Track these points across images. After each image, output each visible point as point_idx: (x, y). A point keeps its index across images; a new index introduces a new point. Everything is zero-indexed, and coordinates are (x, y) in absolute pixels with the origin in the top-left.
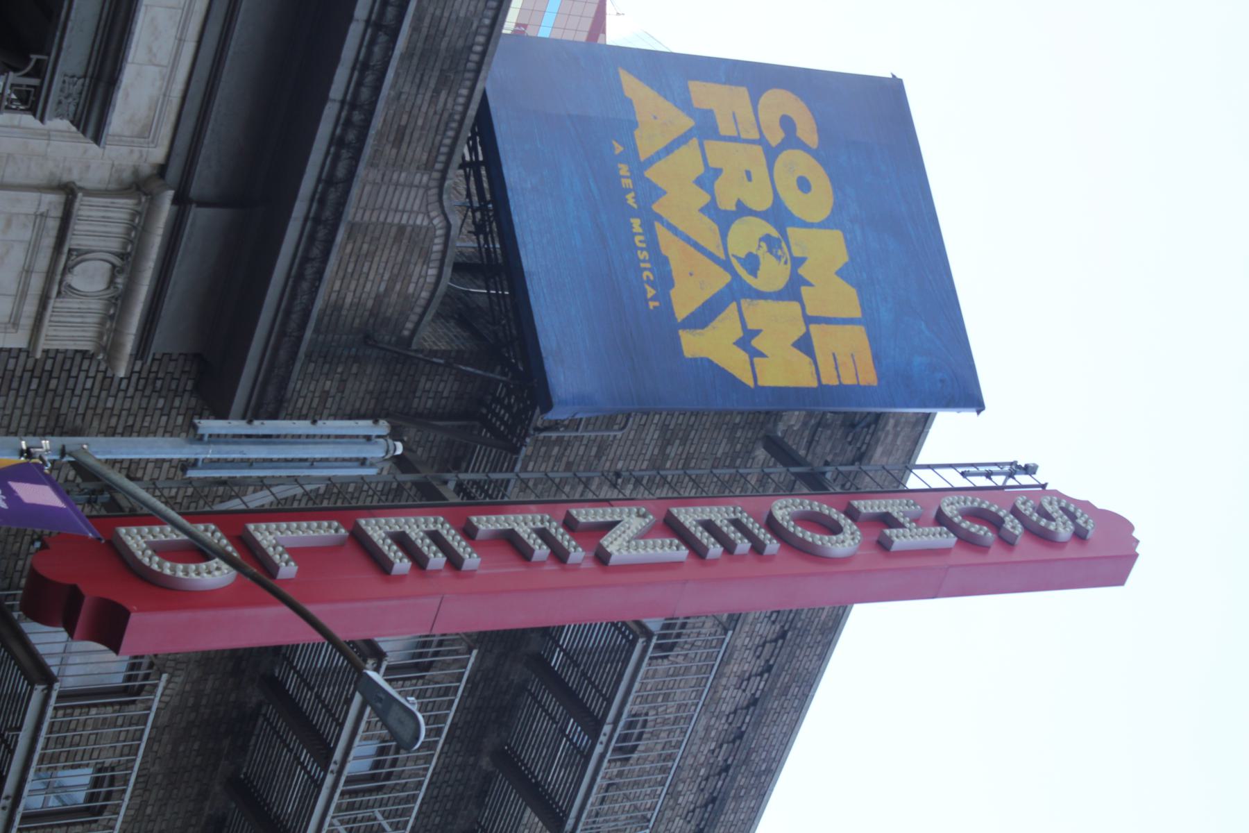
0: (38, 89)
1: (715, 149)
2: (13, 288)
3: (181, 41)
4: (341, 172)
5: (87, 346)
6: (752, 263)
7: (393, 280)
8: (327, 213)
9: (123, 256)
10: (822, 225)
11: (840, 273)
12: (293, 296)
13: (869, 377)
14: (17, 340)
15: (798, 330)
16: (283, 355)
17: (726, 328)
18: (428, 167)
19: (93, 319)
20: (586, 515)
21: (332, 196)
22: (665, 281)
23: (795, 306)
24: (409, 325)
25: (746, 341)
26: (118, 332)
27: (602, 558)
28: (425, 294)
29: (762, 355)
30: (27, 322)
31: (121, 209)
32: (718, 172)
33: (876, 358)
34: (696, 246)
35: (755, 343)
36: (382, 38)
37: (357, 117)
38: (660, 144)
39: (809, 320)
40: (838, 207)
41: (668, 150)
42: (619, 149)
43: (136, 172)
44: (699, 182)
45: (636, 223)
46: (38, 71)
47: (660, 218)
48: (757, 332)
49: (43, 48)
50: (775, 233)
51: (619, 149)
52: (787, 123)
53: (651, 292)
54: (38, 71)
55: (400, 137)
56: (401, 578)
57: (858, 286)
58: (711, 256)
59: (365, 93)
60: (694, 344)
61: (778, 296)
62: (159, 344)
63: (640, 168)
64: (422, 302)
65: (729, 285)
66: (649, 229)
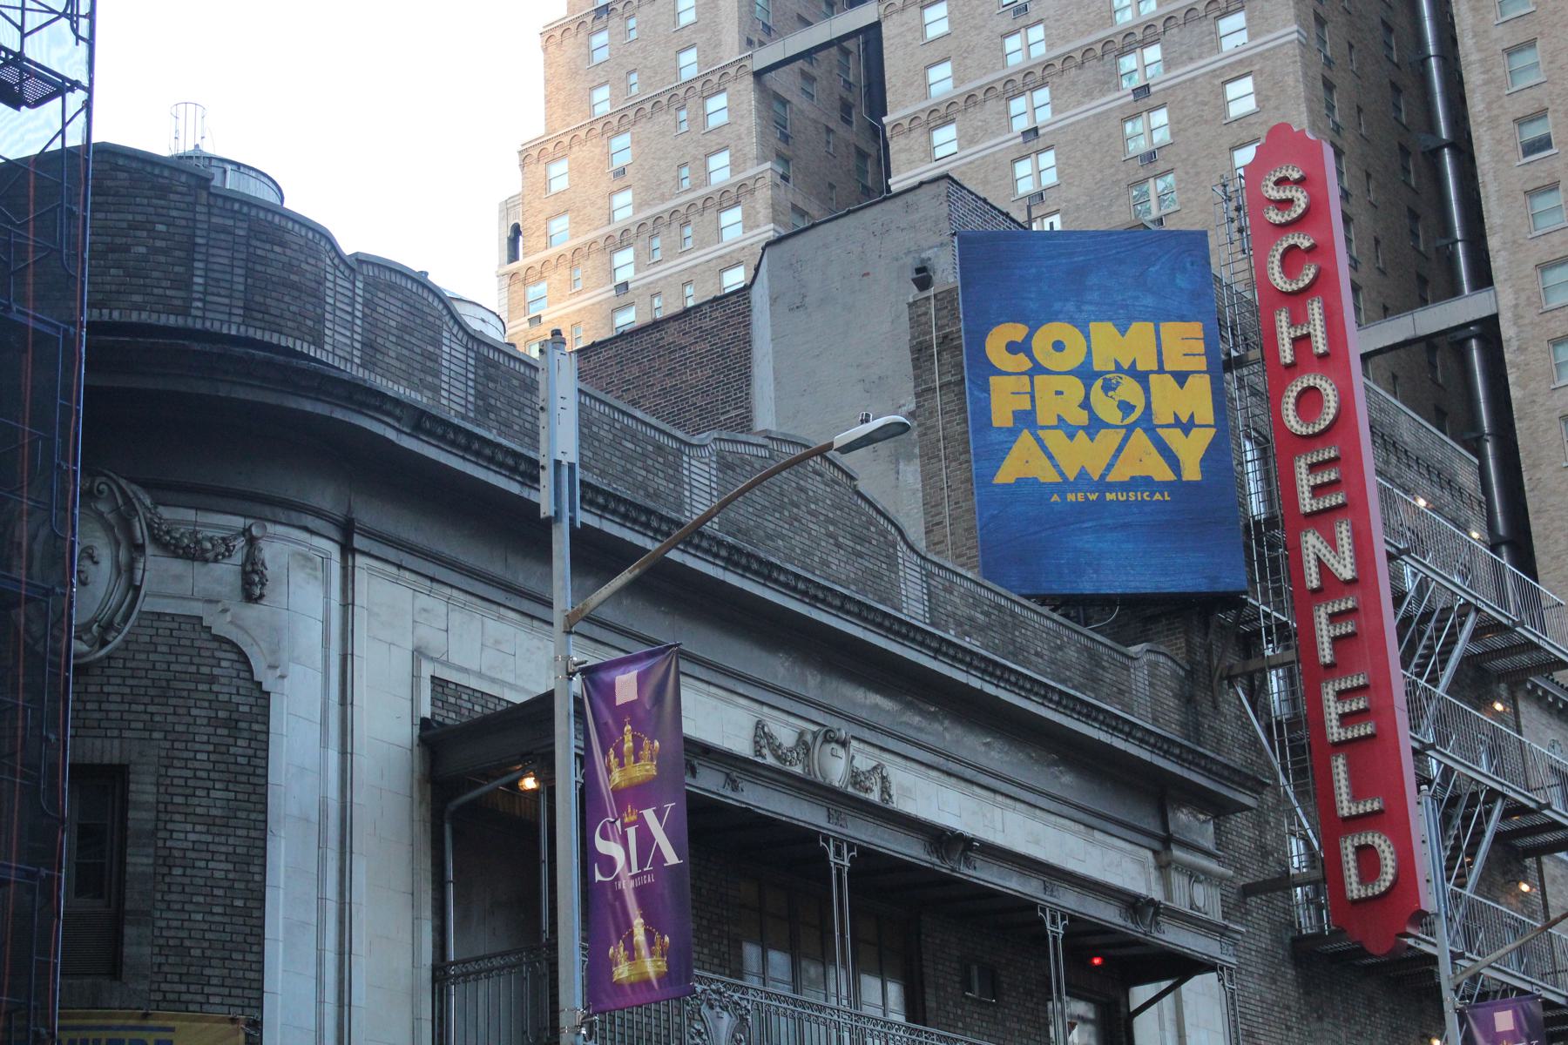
1: (1045, 416)
3: (1114, 847)
4: (1177, 751)
6: (1126, 407)
7: (1168, 687)
9: (1191, 877)
10: (1087, 337)
11: (1123, 332)
12: (1216, 774)
13: (1196, 329)
15: (1171, 382)
17: (1173, 437)
18: (1127, 668)
20: (1313, 581)
22: (1146, 482)
23: (1152, 377)
25: (1187, 427)
27: (1353, 582)
29: (1192, 416)
31: (1178, 880)
32: (1060, 418)
33: (1182, 318)
34: (1120, 450)
35: (1184, 420)
38: (1047, 463)
39: (1161, 370)
40: (1072, 321)
41: (1050, 457)
42: (1055, 498)
44: (1071, 436)
45: (1110, 496)
47: (1103, 476)
48: (1176, 417)
50: (1099, 382)
51: (1055, 498)
52: (1013, 348)
53: (1158, 496)
55: (1121, 692)
56: (1378, 727)
57: (1132, 319)
58: (1125, 439)
59: (1152, 740)
60: (1192, 472)
61: (1147, 390)
62: (1208, 842)
63: (1064, 485)
65: (1145, 430)
66: (1112, 487)
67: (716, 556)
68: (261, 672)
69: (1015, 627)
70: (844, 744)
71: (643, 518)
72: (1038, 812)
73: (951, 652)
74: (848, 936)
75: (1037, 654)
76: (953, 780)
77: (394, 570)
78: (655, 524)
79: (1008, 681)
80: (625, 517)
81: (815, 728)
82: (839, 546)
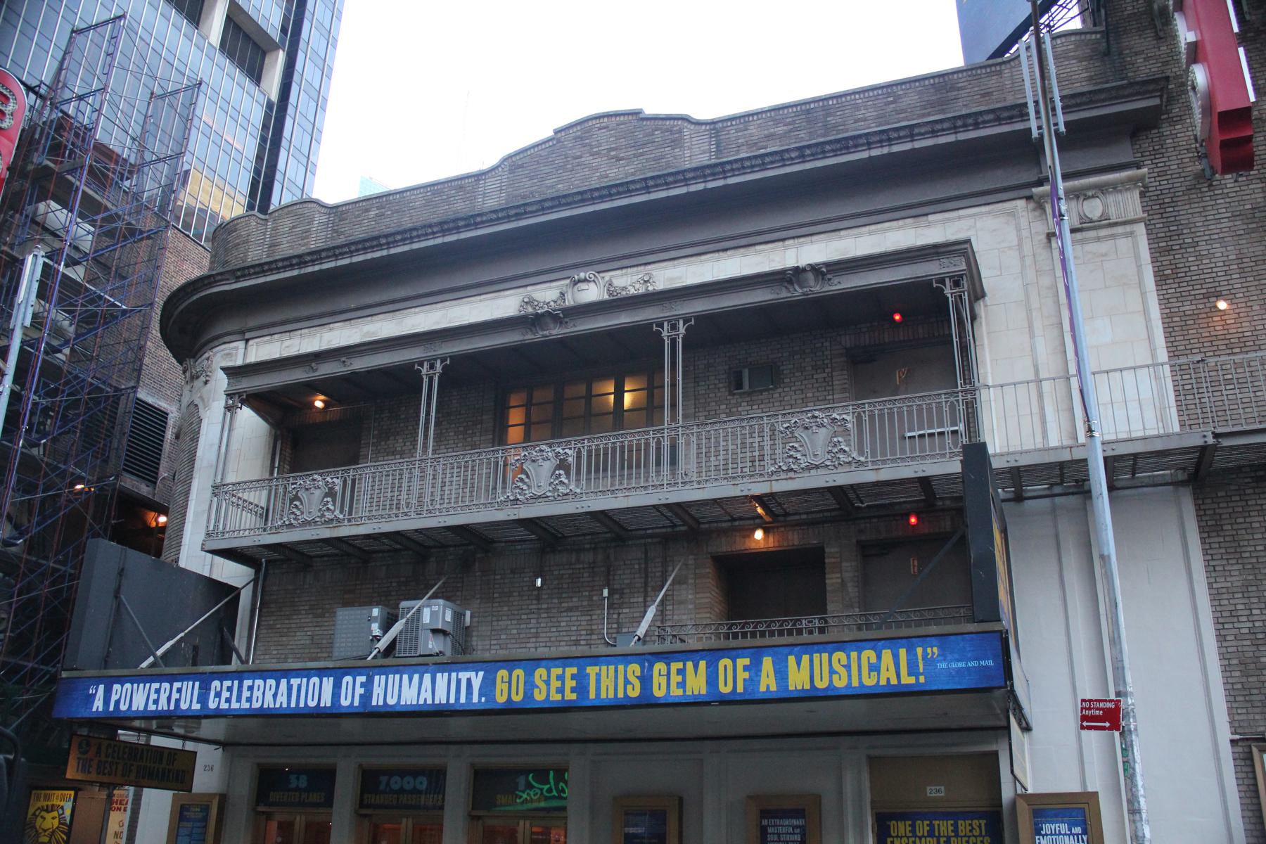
0: (950, 278)
2: (1110, 243)
3: (960, 218)
4: (991, 117)
5: (1136, 194)
7: (1068, 58)
8: (1015, 112)
9: (1078, 197)
14: (1141, 229)
16: (1103, 96)
18: (1000, 73)
19: (1119, 197)
21: (1005, 114)
24: (1093, 37)
26: (1122, 182)
28: (1073, 38)
30: (1128, 228)
36: (916, 131)
37: (959, 123)
43: (1034, 210)
46: (942, 281)
49: (930, 283)
54: (942, 281)
59: (945, 125)
64: (1078, 37)
67: (433, 233)
68: (202, 413)
69: (828, 115)
70: (585, 280)
71: (375, 243)
72: (843, 233)
73: (659, 181)
74: (433, 414)
75: (856, 121)
76: (729, 253)
77: (268, 338)
78: (383, 241)
79: (733, 170)
80: (365, 249)
81: (568, 281)
82: (619, 159)
